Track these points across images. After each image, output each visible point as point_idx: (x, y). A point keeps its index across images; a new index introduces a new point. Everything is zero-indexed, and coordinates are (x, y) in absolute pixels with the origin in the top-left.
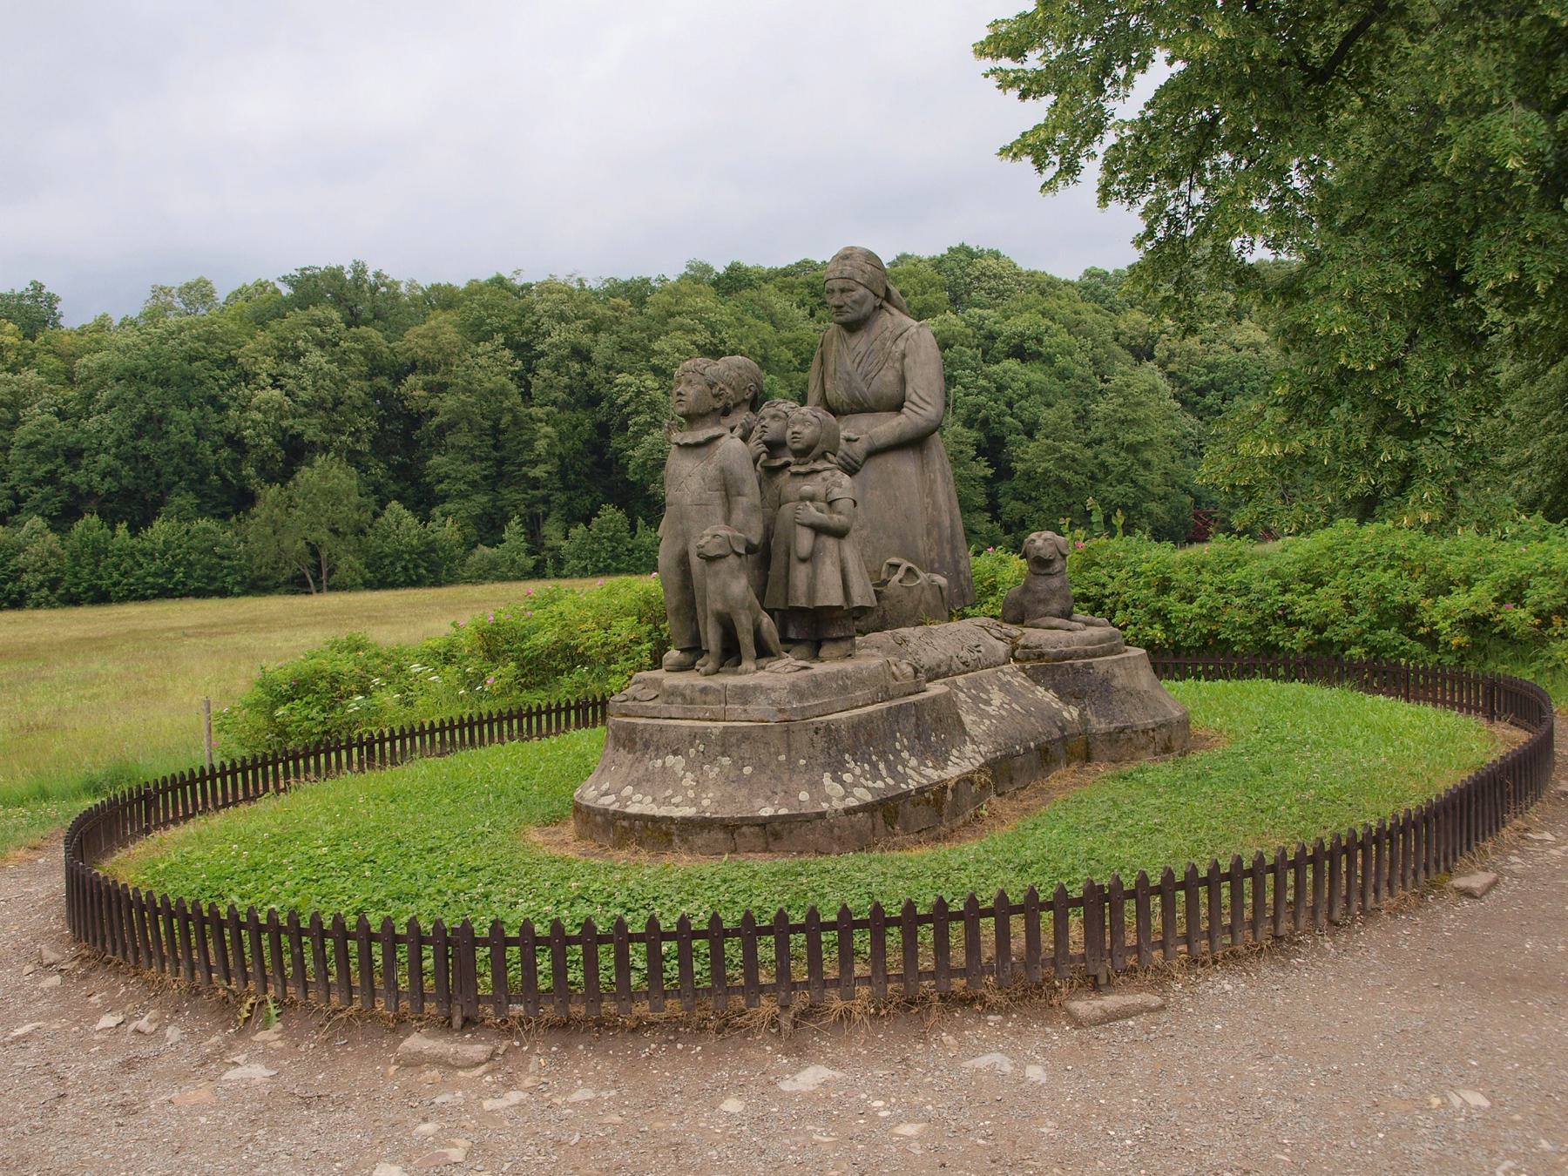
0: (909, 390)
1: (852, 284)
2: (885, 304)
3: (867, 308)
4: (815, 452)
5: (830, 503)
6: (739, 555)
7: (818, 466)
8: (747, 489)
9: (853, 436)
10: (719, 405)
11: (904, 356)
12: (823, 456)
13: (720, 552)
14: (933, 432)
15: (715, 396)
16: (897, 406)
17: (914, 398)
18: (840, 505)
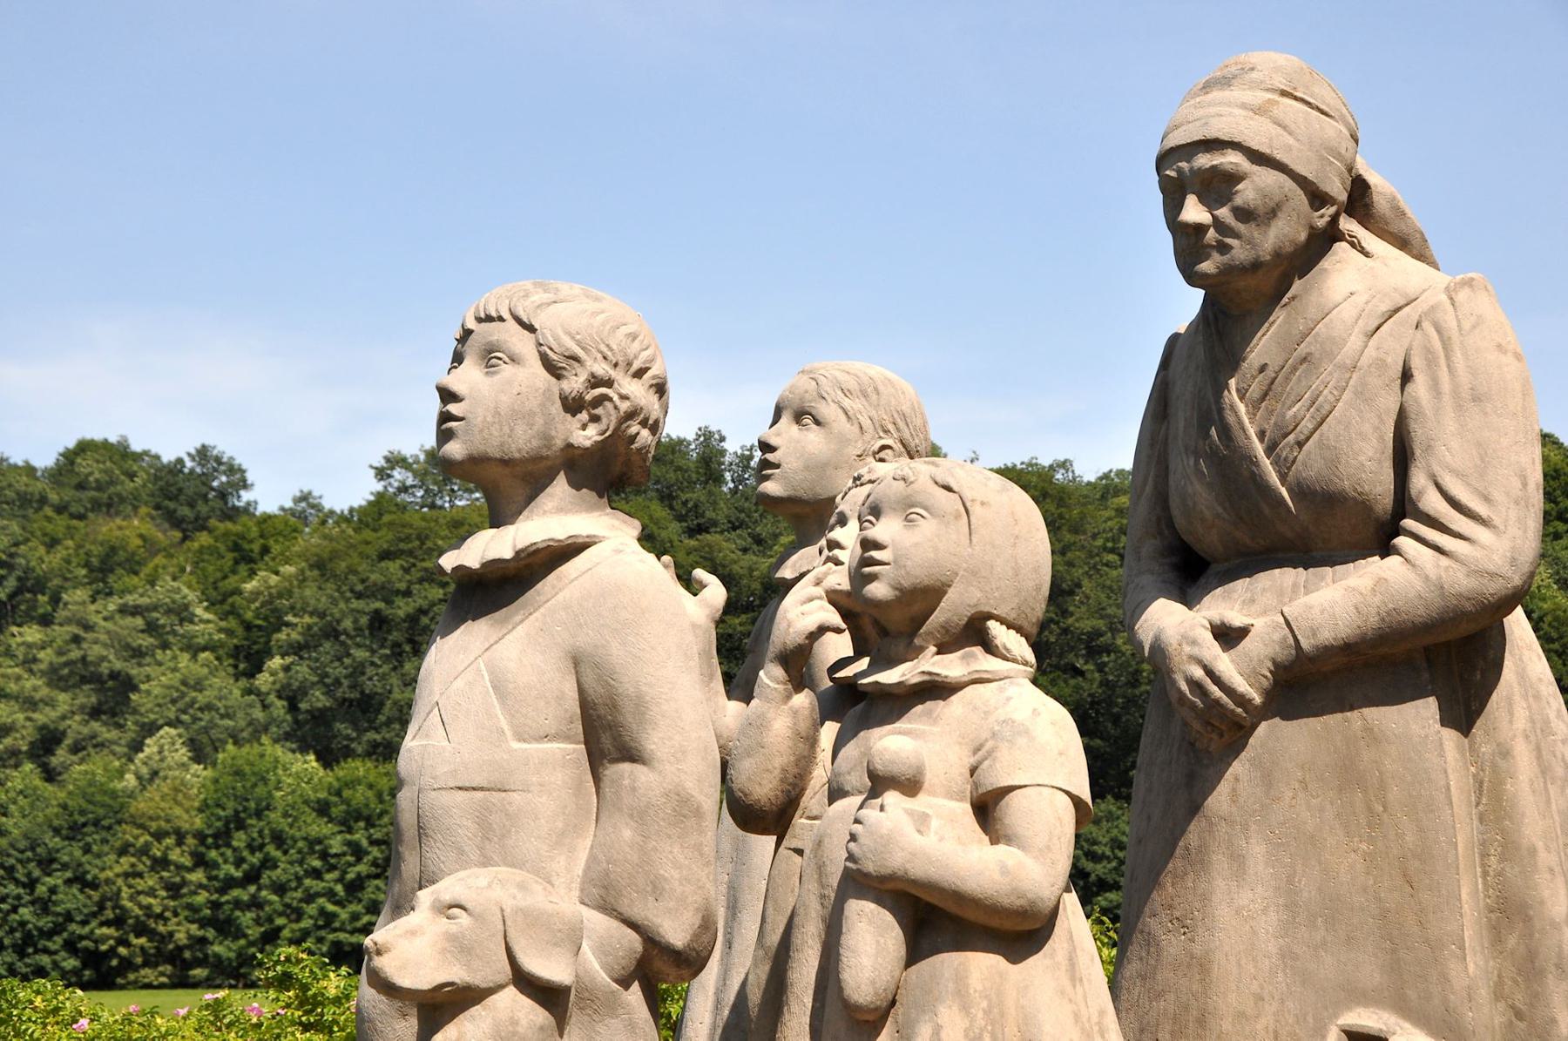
0: (1419, 480)
1: (1232, 159)
2: (1347, 224)
3: (1286, 231)
4: (937, 618)
5: (987, 809)
6: (550, 996)
7: (951, 666)
8: (654, 741)
9: (1237, 619)
10: (587, 436)
11: (1406, 376)
12: (974, 632)
13: (456, 973)
14: (1505, 604)
15: (573, 405)
16: (1380, 537)
17: (1432, 502)
18: (1015, 809)
